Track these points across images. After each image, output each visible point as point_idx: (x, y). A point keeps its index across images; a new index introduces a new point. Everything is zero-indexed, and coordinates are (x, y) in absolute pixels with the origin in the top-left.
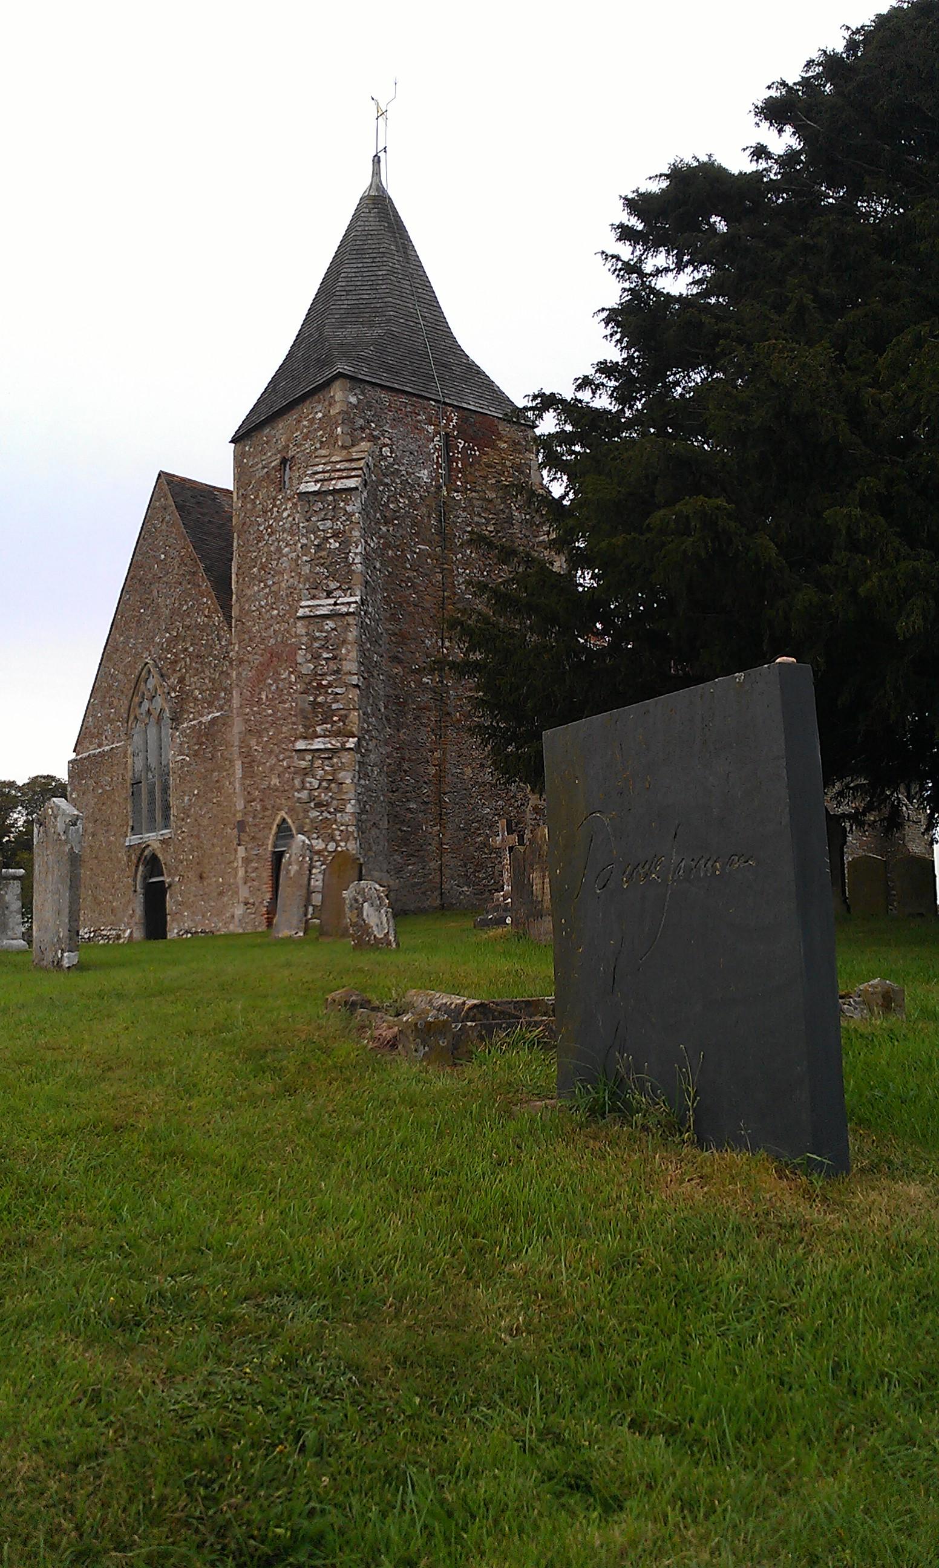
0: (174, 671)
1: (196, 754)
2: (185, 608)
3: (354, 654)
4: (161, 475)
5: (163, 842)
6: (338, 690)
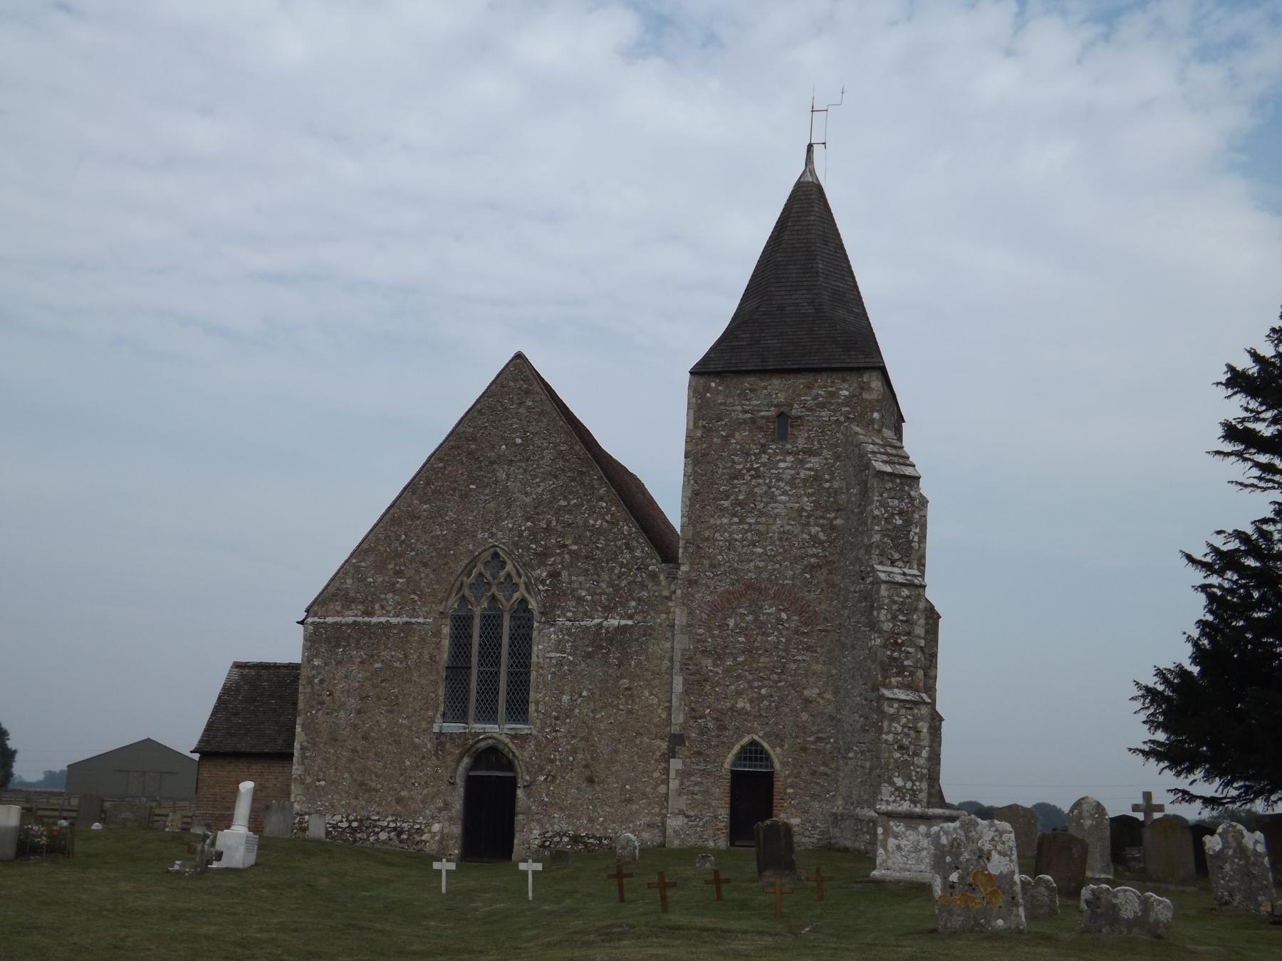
0: (542, 564)
1: (589, 656)
2: (563, 503)
3: (922, 621)
4: (519, 356)
5: (515, 737)
6: (909, 649)
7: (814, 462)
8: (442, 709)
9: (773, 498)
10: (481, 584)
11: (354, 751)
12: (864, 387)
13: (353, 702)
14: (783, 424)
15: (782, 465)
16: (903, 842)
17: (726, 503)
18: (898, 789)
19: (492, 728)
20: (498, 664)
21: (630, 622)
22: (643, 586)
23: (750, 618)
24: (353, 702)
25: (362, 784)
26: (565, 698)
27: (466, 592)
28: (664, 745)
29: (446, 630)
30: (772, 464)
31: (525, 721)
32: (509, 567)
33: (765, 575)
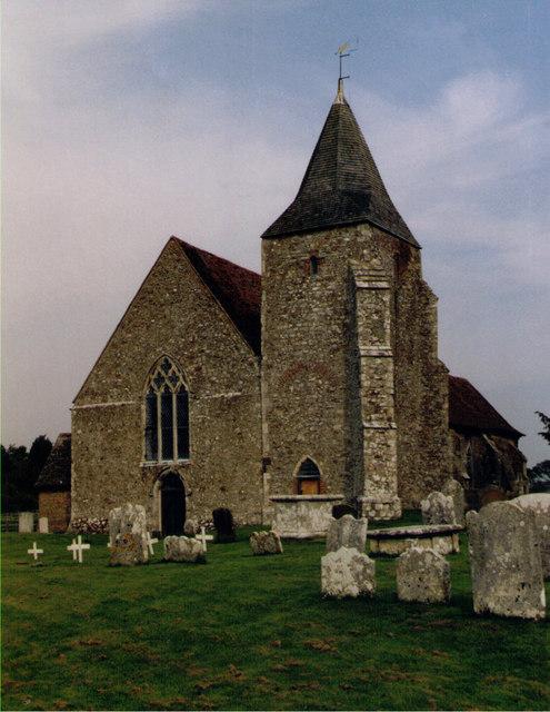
0: (192, 363)
3: (392, 378)
7: (332, 285)
8: (144, 453)
9: (310, 309)
10: (160, 380)
11: (101, 481)
12: (358, 234)
13: (98, 453)
14: (316, 262)
15: (315, 289)
16: (285, 516)
17: (285, 316)
18: (377, 482)
19: (170, 462)
20: (172, 425)
21: (239, 394)
22: (245, 371)
23: (302, 385)
24: (98, 453)
25: (106, 500)
26: (207, 442)
27: (152, 383)
28: (261, 465)
29: (143, 407)
30: (309, 288)
31: (188, 457)
32: (173, 367)
33: (308, 358)
